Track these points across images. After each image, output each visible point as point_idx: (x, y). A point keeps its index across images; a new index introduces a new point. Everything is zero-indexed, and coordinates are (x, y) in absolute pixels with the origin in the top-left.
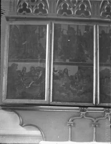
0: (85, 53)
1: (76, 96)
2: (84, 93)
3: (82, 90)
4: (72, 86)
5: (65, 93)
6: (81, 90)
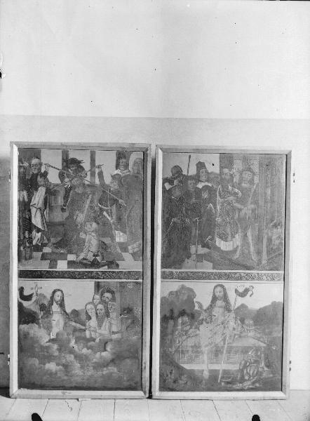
0: (117, 240)
1: (90, 372)
2: (113, 361)
3: (106, 352)
4: (76, 342)
5: (58, 364)
6: (104, 354)
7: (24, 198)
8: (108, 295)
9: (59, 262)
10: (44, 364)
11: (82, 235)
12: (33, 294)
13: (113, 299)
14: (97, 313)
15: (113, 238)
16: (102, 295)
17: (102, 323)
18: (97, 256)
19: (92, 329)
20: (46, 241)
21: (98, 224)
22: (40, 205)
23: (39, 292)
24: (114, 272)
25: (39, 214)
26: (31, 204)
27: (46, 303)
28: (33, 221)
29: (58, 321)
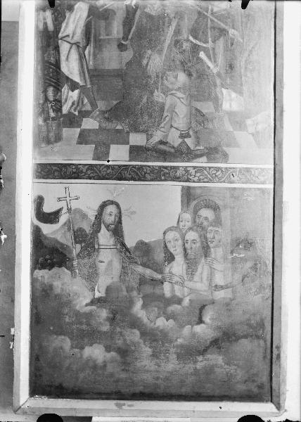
0: (226, 106)
1: (171, 365)
2: (215, 343)
3: (203, 325)
4: (144, 306)
5: (108, 349)
6: (199, 329)
7: (45, 24)
8: (206, 213)
9: (113, 148)
10: (82, 348)
11: (158, 96)
12: (60, 210)
14: (185, 250)
15: (217, 102)
16: (196, 212)
18: (188, 136)
19: (176, 279)
20: (88, 107)
21: (190, 75)
22: (78, 36)
23: (74, 205)
24: (218, 169)
25: (74, 56)
26: (60, 35)
27: (87, 229)
28: (64, 69)
29: (111, 261)
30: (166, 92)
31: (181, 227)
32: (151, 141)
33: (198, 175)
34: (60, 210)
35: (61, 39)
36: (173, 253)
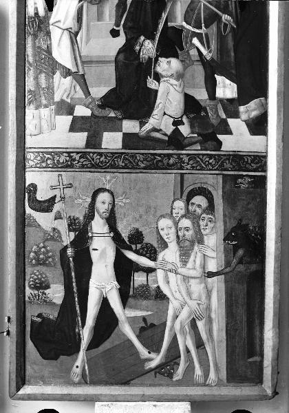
7: (36, 9)
8: (200, 200)
9: (106, 135)
11: (152, 84)
12: (55, 196)
13: (211, 208)
14: (178, 237)
17: (189, 256)
18: (182, 123)
22: (70, 22)
24: (210, 156)
26: (51, 21)
28: (56, 54)
29: (105, 249)
30: (158, 77)
31: (174, 215)
32: (143, 129)
33: (191, 162)
34: (55, 196)
35: (52, 25)
36: (167, 240)
